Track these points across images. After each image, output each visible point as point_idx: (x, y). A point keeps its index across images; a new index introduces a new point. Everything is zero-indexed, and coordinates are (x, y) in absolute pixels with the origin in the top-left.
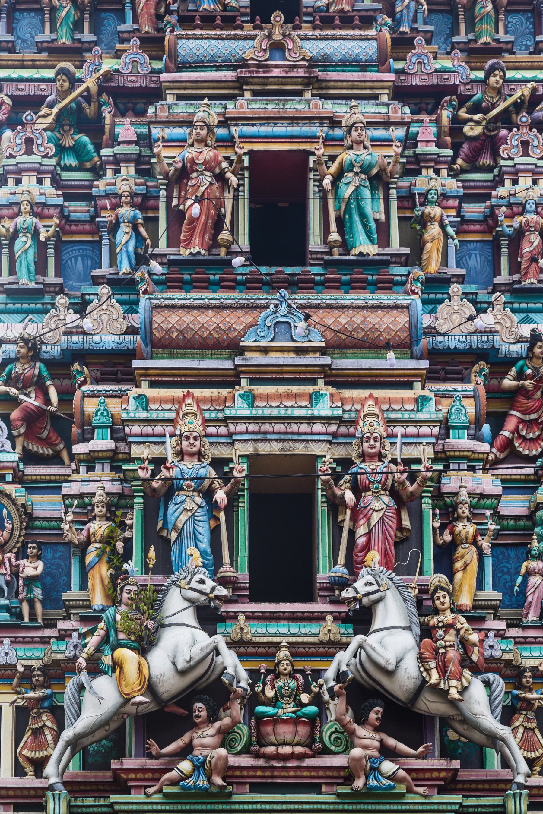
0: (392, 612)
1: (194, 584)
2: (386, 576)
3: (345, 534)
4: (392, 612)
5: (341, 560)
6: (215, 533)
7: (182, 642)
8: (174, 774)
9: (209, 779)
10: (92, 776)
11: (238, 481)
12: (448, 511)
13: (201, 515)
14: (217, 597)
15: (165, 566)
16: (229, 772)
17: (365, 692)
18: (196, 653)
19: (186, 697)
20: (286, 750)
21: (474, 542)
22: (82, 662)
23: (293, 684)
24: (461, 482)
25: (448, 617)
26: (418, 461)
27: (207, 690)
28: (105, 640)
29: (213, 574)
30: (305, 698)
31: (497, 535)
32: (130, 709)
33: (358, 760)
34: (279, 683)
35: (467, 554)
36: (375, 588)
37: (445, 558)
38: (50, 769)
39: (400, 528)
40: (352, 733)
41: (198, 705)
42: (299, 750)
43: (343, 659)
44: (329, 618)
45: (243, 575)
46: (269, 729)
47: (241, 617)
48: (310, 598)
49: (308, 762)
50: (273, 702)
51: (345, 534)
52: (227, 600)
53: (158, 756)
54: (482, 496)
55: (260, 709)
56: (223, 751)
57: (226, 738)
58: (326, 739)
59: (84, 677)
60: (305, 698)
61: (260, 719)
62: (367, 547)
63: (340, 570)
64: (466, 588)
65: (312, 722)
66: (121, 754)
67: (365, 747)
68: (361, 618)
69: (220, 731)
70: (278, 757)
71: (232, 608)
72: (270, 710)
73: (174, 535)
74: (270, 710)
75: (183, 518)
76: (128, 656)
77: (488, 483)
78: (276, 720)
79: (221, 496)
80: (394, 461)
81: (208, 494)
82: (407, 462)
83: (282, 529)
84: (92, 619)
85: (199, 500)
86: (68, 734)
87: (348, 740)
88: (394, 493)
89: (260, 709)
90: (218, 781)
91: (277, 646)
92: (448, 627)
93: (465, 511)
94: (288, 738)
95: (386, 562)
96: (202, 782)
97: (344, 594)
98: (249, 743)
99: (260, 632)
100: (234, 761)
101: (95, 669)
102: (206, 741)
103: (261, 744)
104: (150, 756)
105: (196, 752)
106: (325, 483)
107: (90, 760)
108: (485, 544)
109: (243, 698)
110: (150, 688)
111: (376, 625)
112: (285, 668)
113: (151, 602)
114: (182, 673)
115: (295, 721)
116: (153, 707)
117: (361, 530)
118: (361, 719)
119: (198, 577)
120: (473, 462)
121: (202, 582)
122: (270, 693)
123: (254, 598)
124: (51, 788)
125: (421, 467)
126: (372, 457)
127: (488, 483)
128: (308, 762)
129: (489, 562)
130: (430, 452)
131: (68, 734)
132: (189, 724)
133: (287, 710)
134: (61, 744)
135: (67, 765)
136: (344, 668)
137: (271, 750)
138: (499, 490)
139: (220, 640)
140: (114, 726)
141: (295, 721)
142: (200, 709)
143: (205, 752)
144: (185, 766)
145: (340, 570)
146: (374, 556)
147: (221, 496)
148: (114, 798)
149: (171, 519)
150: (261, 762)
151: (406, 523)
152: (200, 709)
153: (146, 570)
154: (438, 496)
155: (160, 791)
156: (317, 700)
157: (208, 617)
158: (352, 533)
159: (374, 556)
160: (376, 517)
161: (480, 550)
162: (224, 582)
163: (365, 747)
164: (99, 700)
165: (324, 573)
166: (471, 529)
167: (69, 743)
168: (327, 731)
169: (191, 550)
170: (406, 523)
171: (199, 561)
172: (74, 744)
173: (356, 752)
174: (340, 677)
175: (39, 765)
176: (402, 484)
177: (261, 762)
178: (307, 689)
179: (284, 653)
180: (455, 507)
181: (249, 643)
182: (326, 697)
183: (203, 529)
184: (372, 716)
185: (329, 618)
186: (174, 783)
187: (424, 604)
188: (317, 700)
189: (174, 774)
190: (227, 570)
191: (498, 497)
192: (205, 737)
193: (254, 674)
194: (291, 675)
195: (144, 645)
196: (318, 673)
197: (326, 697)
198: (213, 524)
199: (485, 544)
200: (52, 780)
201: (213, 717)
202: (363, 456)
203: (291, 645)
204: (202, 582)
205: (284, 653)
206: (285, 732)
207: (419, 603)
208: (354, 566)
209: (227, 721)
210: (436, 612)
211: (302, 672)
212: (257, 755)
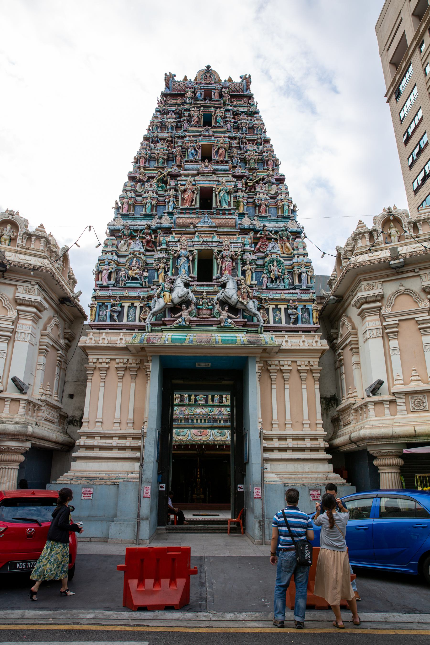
0: (231, 285)
1: (183, 277)
2: (229, 276)
3: (220, 267)
4: (231, 285)
5: (219, 273)
6: (189, 267)
7: (180, 290)
8: (177, 322)
9: (186, 323)
10: (157, 322)
11: (195, 255)
12: (244, 263)
13: (186, 262)
14: (189, 280)
15: (177, 273)
16: (190, 321)
17: (223, 303)
18: (183, 293)
19: (180, 304)
20: (205, 316)
21: (251, 270)
22: (156, 295)
23: (207, 301)
24: (248, 257)
25: (244, 286)
26: (237, 251)
27: (186, 302)
28: (162, 290)
29: (188, 276)
30: (209, 304)
31: (256, 269)
32: (167, 306)
33: (222, 319)
34: (203, 301)
35: (249, 273)
36: (227, 279)
37: (244, 273)
38: (147, 320)
39: (233, 266)
40: (221, 313)
41: (183, 305)
42: (208, 316)
43: (219, 295)
44: (216, 286)
45: (196, 276)
46: (201, 311)
47: (195, 285)
48: (212, 281)
49: (210, 319)
50: (202, 305)
51: (220, 267)
52: (191, 282)
53: (174, 317)
54: (252, 260)
55: (199, 306)
56: (189, 316)
57: (190, 313)
58: (214, 314)
59: (156, 298)
60: (209, 304)
61: (198, 309)
62: (225, 270)
63: (218, 275)
64: (249, 280)
65: (211, 310)
66: (165, 316)
67: (224, 316)
68: (223, 286)
69: (189, 312)
70: (203, 318)
71: (193, 283)
72: (201, 307)
73: (179, 267)
74: (201, 307)
75: (181, 263)
76: (167, 294)
77: (254, 257)
78: (202, 309)
79: (191, 258)
80: (232, 251)
81: (188, 258)
82: (235, 251)
83: (205, 266)
84: (159, 286)
85: (185, 259)
86: (151, 312)
87: (220, 314)
88: (231, 258)
89: (199, 306)
90: (188, 323)
91: (203, 292)
92: (244, 288)
93: (248, 263)
94: (205, 313)
95: (229, 273)
96: (184, 324)
97: (219, 280)
98: (196, 315)
99: (199, 289)
100: (192, 319)
101: (159, 297)
102: (185, 314)
103: (199, 315)
104: (171, 317)
105: (183, 316)
106: (215, 255)
107: (157, 319)
108: (253, 270)
109: (194, 304)
110: (172, 301)
111: (227, 288)
112: (205, 297)
113: (173, 281)
114: (180, 298)
115: (207, 309)
116: (172, 306)
117: (224, 266)
118: (223, 309)
119: (184, 276)
120: (250, 252)
121: (185, 277)
122: (201, 303)
123: (198, 281)
124: (147, 324)
125: (238, 252)
126: (226, 250)
127: (254, 257)
128: (210, 319)
129: (254, 274)
130: (240, 249)
131: (151, 312)
132: (181, 310)
133: (205, 307)
134: (150, 314)
135: (152, 319)
136: (219, 297)
137: (201, 316)
138: (256, 258)
139: (189, 290)
140: (163, 310)
141: (207, 309)
142: (184, 306)
143: (185, 316)
144: (180, 320)
145: (218, 275)
146: (227, 272)
147: (191, 258)
148: (162, 327)
149: (179, 263)
150: (198, 319)
151: (234, 265)
152: (184, 306)
153: (172, 274)
154: (242, 259)
155: (174, 326)
156: (212, 305)
157: (187, 285)
158: (221, 267)
159: (227, 272)
160: (227, 263)
161: (252, 271)
162: (191, 277)
163: (224, 316)
164: (159, 304)
165: (215, 275)
166: (250, 267)
167: (152, 314)
168: (215, 312)
169: (183, 270)
170: (234, 265)
171: (185, 272)
172: (154, 314)
173: (222, 317)
174: (218, 299)
175: (145, 319)
176: (233, 256)
177: (198, 319)
178: (210, 302)
179: (205, 294)
180: (246, 262)
181: (196, 291)
182: (215, 304)
183: (186, 266)
184: (226, 308)
185: (216, 286)
186: (177, 324)
187: (238, 283)
188: (212, 305)
189: (177, 322)
190: (191, 275)
191: (256, 260)
192: (185, 313)
193: (197, 298)
194: (206, 299)
195: (171, 291)
196: (213, 299)
197: (215, 304)
198: (189, 264)
199: (253, 270)
200: (147, 323)
201: (187, 308)
202: (224, 250)
203: (206, 292)
204: (185, 277)
205: (205, 294)
206: (205, 312)
207: (237, 283)
208: (221, 274)
209: (190, 309)
210: (241, 285)
211: (209, 298)
212: (198, 318)
